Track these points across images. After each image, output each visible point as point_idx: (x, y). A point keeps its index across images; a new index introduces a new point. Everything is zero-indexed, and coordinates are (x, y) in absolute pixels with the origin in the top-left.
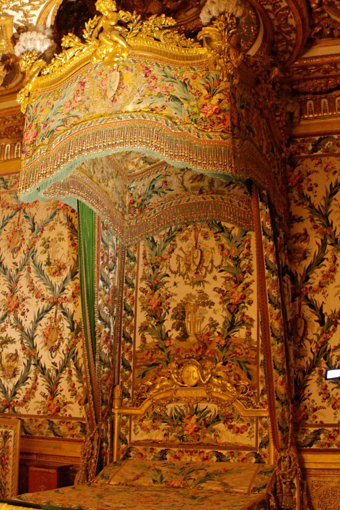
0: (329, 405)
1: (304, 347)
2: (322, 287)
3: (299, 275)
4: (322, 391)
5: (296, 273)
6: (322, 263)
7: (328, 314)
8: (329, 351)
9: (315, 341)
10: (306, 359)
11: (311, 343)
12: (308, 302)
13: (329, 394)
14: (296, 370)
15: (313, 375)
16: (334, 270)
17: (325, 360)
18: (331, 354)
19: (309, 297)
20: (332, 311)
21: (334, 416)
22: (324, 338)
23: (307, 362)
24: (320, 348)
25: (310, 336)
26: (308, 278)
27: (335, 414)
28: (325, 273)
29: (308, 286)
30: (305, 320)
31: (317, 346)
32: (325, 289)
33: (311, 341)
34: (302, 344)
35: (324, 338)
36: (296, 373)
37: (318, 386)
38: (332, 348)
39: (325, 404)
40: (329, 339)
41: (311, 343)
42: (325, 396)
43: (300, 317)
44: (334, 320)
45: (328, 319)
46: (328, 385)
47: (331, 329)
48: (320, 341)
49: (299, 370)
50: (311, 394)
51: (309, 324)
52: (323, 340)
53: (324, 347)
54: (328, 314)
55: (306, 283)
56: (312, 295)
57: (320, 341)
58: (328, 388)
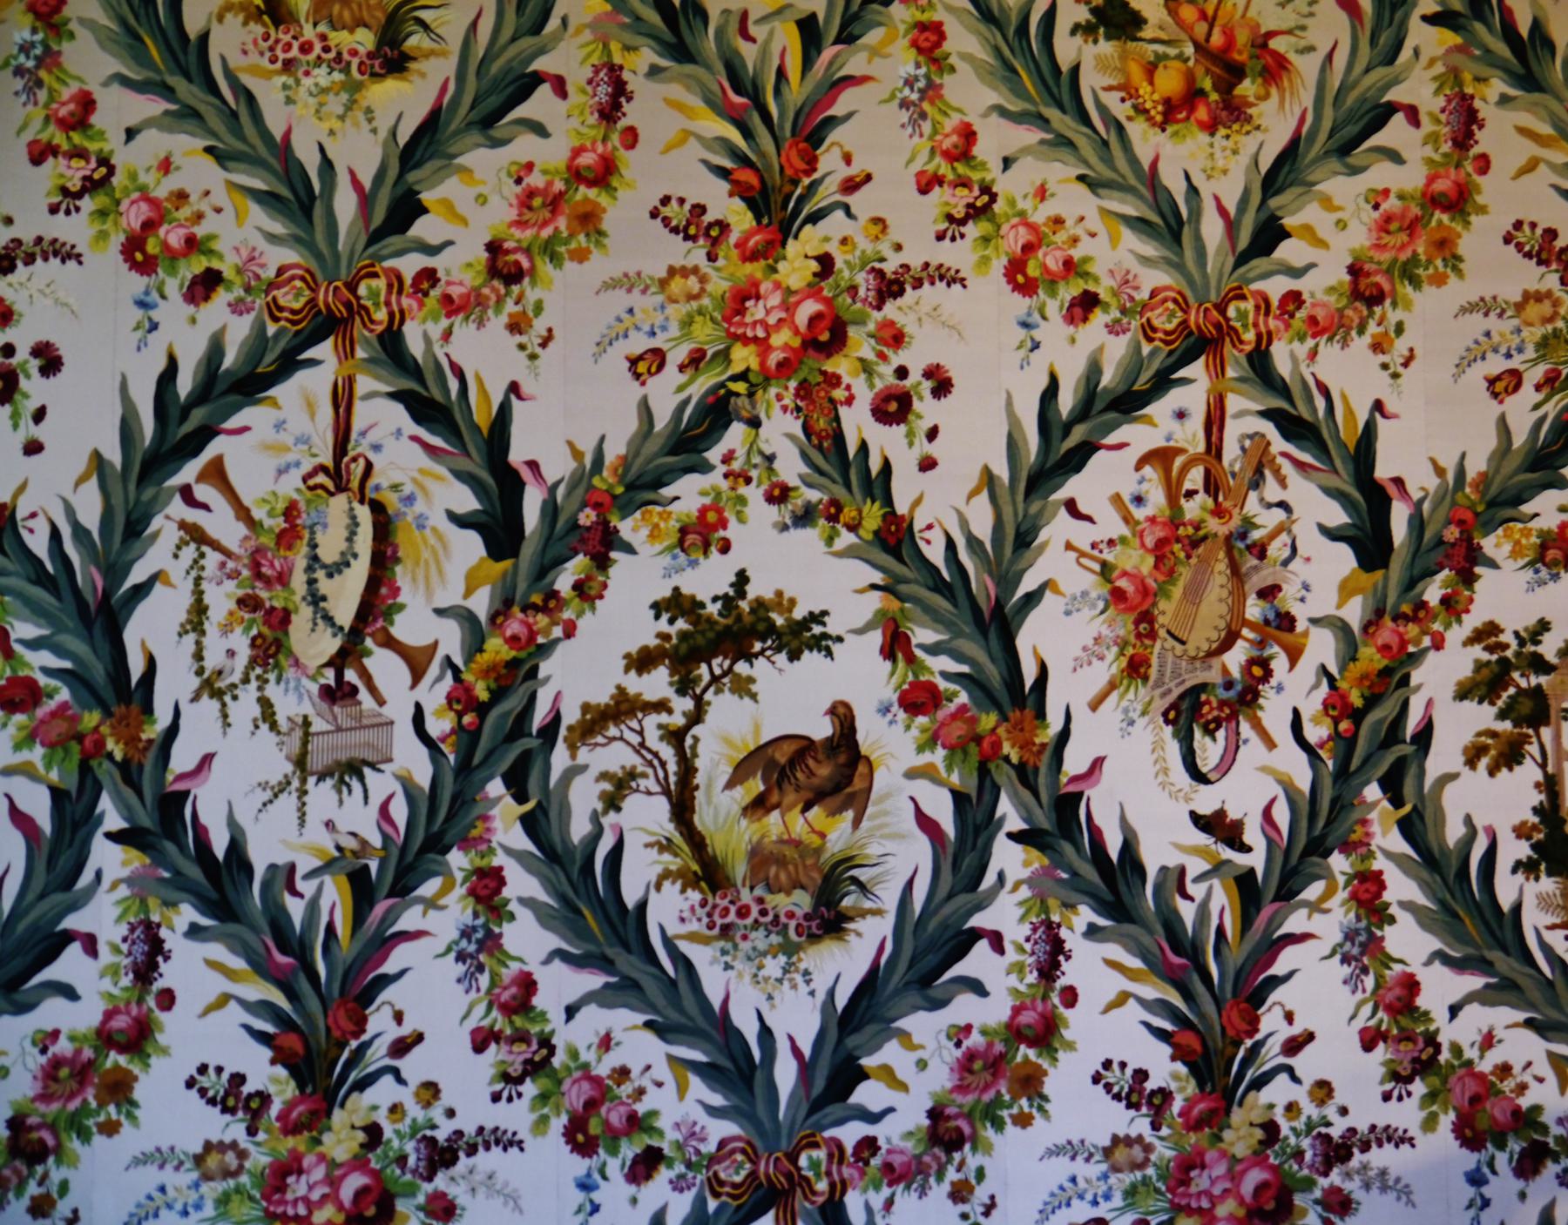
0: (541, 1124)
1: (364, 695)
2: (513, 276)
3: (343, 180)
4: (498, 1020)
5: (327, 165)
6: (520, 112)
7: (551, 475)
8: (550, 731)
9: (448, 661)
10: (381, 784)
11: (417, 676)
12: (409, 384)
13: (546, 1043)
14: (305, 864)
15: (431, 904)
16: (604, 174)
17: (521, 798)
18: (560, 758)
19: (415, 345)
20: (577, 454)
21: (579, 1197)
22: (513, 641)
23: (384, 810)
24: (482, 709)
25: (412, 626)
26: (407, 209)
27: (585, 1186)
28: (536, 180)
29: (410, 265)
30: (377, 508)
31: (461, 699)
32: (532, 295)
33: (417, 662)
34: (351, 675)
35: (513, 641)
36: (307, 887)
37: (468, 980)
38: (571, 716)
39: (516, 1116)
40: (545, 650)
41: (417, 676)
42: (515, 1058)
43: (341, 487)
44: (587, 517)
45: (551, 510)
46: (540, 974)
47: (564, 582)
48: (484, 659)
49: (328, 866)
50: (419, 1038)
51: (404, 538)
52: (507, 653)
53: (512, 703)
54: (551, 475)
55: (395, 241)
56: (435, 330)
57: (484, 659)
58: (538, 1001)
